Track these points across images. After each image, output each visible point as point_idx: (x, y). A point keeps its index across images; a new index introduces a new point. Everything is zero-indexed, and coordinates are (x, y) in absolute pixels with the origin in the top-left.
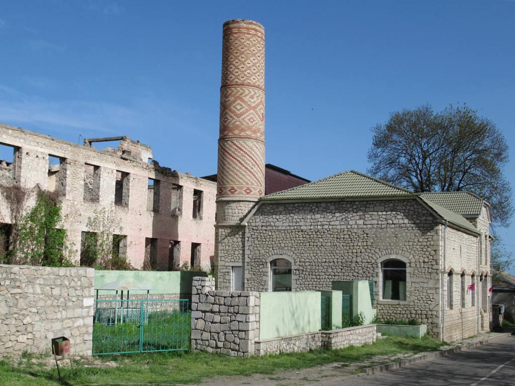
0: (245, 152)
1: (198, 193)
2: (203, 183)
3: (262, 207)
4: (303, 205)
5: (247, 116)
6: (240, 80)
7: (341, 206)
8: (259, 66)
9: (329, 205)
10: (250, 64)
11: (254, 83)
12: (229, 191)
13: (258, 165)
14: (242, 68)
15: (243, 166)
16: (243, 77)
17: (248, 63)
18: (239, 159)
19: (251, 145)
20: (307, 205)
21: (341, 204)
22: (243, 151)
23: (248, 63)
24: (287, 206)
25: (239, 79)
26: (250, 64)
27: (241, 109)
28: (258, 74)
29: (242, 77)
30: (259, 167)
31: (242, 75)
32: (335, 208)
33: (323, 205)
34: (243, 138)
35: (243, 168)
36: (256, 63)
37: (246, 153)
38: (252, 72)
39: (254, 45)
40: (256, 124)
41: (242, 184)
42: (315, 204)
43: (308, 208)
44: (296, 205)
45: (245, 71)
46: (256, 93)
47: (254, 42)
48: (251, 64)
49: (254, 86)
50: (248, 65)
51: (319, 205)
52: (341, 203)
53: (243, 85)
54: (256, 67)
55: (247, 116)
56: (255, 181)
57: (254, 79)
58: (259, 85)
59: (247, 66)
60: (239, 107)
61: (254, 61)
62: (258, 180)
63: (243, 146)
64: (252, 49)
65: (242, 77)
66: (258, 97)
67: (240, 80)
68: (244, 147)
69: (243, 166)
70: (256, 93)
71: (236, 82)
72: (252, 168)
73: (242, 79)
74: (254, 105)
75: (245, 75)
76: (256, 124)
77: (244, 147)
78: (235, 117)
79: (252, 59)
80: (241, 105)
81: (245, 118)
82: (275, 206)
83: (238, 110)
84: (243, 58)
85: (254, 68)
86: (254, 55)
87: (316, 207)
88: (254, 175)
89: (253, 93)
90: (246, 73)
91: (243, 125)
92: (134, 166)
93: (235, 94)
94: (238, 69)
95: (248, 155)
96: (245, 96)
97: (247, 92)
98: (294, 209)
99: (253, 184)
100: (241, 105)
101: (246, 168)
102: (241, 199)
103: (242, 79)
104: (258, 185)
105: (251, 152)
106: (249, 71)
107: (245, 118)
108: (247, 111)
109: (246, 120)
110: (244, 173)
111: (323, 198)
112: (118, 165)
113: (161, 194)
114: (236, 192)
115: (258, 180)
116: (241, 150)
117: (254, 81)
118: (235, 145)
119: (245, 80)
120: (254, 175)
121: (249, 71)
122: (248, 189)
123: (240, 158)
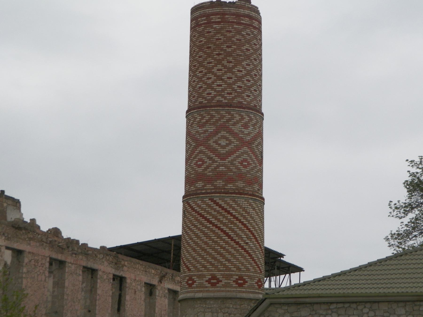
0: (234, 217)
1: (120, 281)
2: (126, 263)
3: (269, 309)
4: (346, 305)
5: (238, 157)
6: (225, 98)
7: (415, 308)
8: (256, 75)
9: (394, 306)
10: (241, 71)
11: (249, 103)
12: (206, 281)
13: (256, 238)
14: (229, 78)
15: (232, 239)
16: (230, 94)
17: (239, 71)
18: (225, 228)
19: (245, 204)
20: (354, 306)
21: (416, 305)
22: (231, 214)
23: (239, 71)
24: (316, 307)
25: (223, 97)
26: (241, 71)
27: (227, 145)
28: (255, 87)
29: (228, 94)
30: (257, 241)
31: (229, 90)
32: (406, 312)
33: (384, 307)
34: (231, 193)
35: (232, 243)
36: (252, 70)
37: (237, 219)
38: (245, 85)
39: (249, 42)
40: (252, 169)
41: (230, 270)
42: (368, 305)
43: (355, 312)
44: (332, 307)
45: (234, 83)
46: (251, 120)
47: (248, 37)
48: (244, 72)
49: (249, 108)
50: (239, 74)
51: (375, 306)
52: (418, 303)
53: (230, 106)
54: (251, 76)
55: (238, 157)
56: (251, 264)
57: (249, 96)
58: (255, 106)
59: (236, 76)
60: (223, 142)
61: (248, 68)
62: (256, 263)
63: (231, 206)
64: (244, 48)
65: (228, 94)
66: (254, 125)
67: (225, 98)
68: (234, 209)
69: (232, 239)
70: (251, 120)
71: (218, 101)
72: (247, 243)
73: (229, 97)
74: (248, 138)
75: (233, 89)
76: (252, 169)
77: (234, 209)
78: (216, 159)
79: (244, 63)
80: (227, 139)
81: (235, 160)
82: (293, 308)
83: (223, 147)
84: (231, 62)
85: (248, 77)
86: (248, 57)
87: (371, 309)
88: (250, 255)
89: (247, 119)
90: (235, 87)
91: (231, 171)
92: (30, 239)
93: (217, 121)
94: (222, 80)
95: (240, 222)
96: (234, 124)
97: (238, 117)
98: (330, 312)
99: (248, 270)
100: (227, 139)
101: (237, 243)
102: (229, 295)
103: (229, 97)
104: (256, 272)
105: (244, 217)
106: (239, 84)
107: (235, 160)
108: (238, 148)
109: (236, 163)
110: (232, 251)
111: (385, 295)
112: (8, 239)
113: (66, 284)
114: (220, 284)
115: (256, 263)
116: (229, 212)
117: (249, 99)
118: (217, 204)
119: (233, 98)
120: (250, 255)
121: (239, 84)
122: (241, 278)
123: (227, 226)
